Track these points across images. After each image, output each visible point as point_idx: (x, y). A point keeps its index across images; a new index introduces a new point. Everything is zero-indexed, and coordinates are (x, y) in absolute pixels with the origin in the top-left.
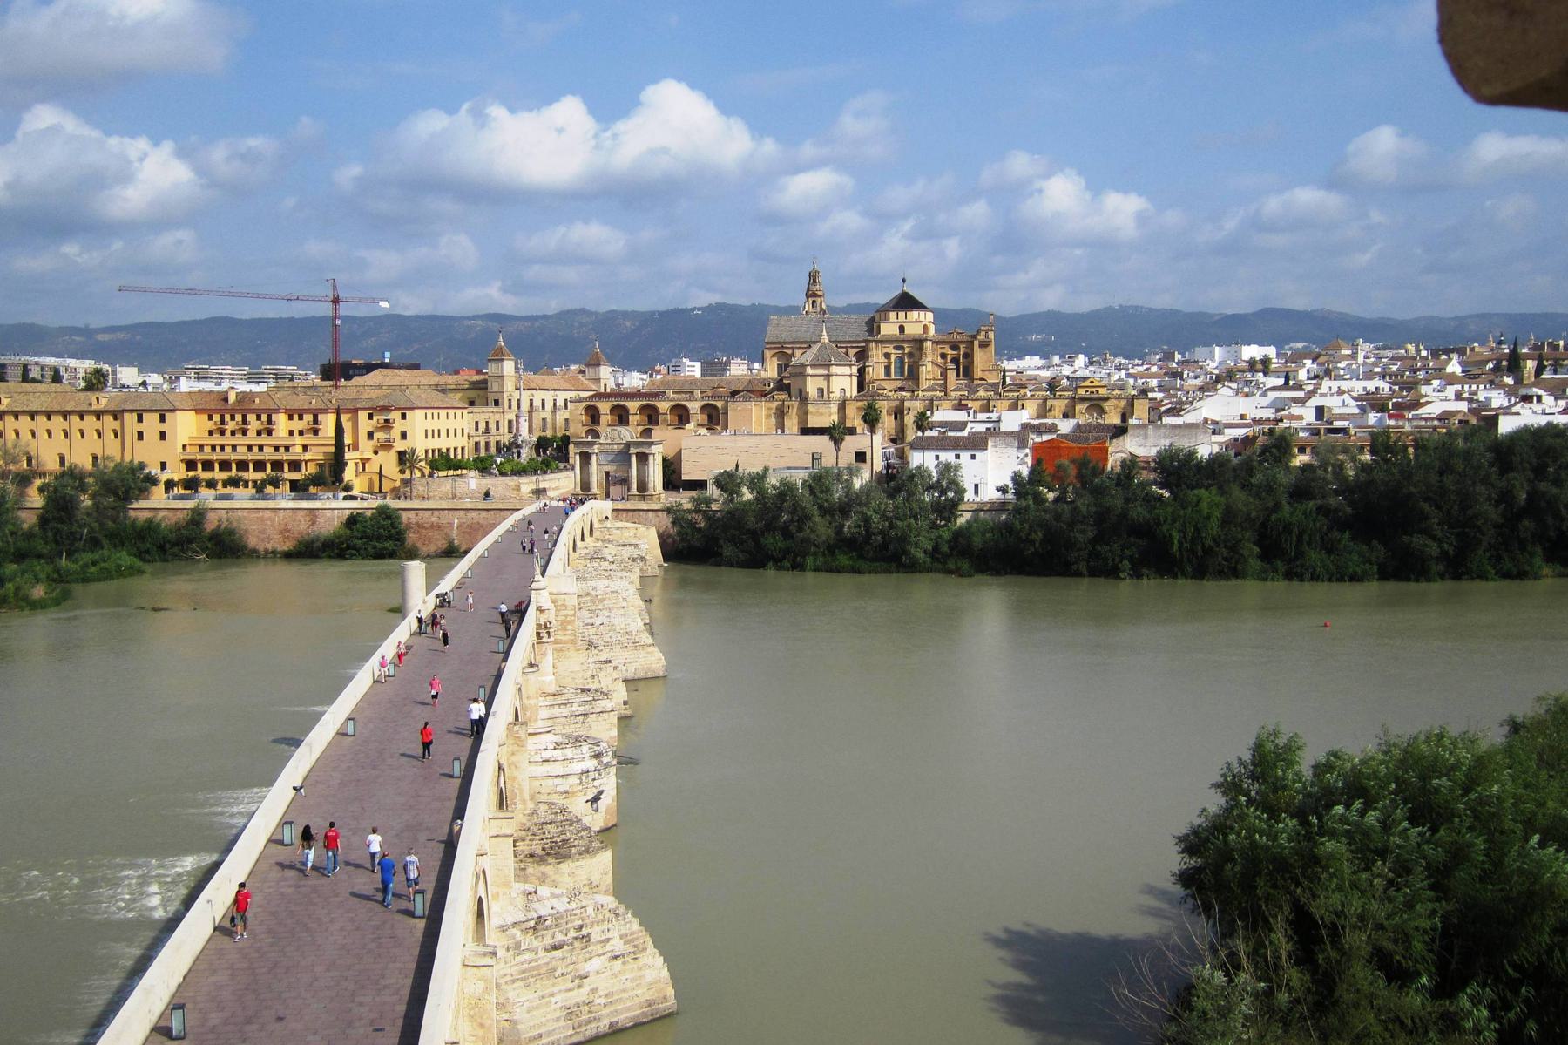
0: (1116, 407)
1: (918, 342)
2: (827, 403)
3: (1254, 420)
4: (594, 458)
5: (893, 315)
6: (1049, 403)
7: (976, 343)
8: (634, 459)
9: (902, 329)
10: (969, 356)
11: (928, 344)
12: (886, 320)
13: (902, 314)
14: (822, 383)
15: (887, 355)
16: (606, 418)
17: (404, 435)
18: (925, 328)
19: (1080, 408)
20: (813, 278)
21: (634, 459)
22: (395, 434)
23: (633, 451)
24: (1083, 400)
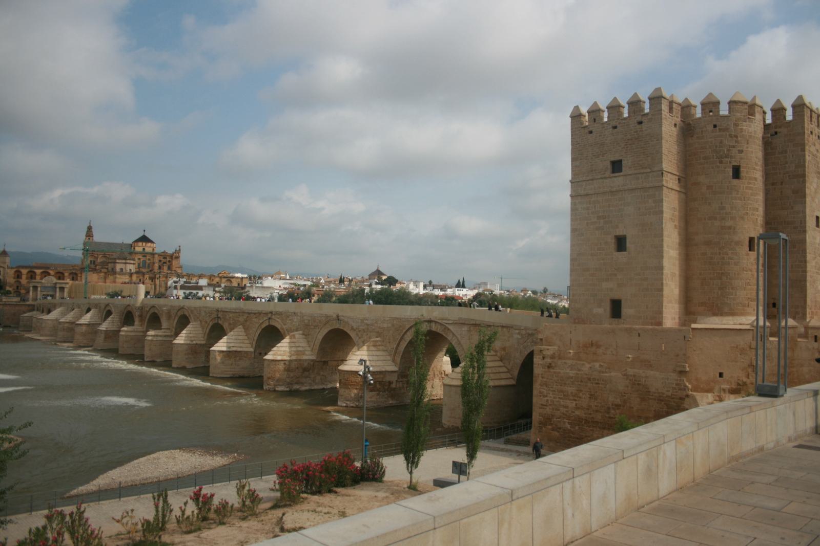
0: (236, 281)
3: (284, 288)
4: (39, 289)
5: (140, 244)
7: (174, 257)
8: (58, 290)
9: (144, 249)
13: (144, 244)
14: (122, 266)
15: (139, 259)
16: (24, 277)
19: (224, 280)
20: (90, 228)
21: (58, 290)
23: (58, 286)
24: (224, 277)
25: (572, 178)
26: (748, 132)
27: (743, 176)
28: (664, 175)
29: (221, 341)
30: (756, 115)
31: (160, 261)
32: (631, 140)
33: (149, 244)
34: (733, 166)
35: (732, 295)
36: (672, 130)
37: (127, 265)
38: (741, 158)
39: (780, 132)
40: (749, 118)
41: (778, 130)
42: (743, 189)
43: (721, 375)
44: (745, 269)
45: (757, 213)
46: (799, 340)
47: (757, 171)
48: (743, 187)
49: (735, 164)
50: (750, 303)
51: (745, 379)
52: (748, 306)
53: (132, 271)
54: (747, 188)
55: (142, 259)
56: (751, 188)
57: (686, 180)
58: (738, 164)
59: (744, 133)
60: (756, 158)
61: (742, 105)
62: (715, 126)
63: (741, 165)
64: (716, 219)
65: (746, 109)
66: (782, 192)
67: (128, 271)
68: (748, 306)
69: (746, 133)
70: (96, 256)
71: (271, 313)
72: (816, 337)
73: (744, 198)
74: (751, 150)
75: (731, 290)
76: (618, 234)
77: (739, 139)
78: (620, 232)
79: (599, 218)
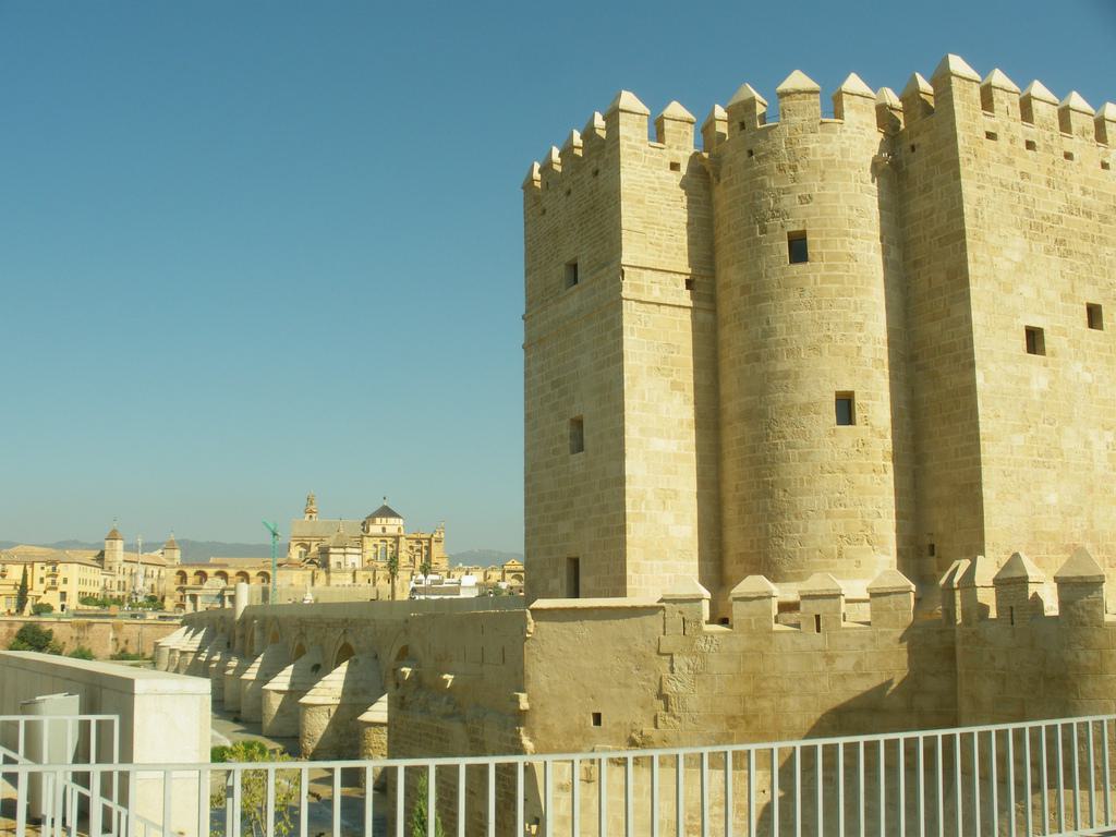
1: (397, 539)
2: (344, 572)
5: (378, 520)
6: (488, 574)
7: (433, 539)
8: (227, 599)
9: (384, 529)
10: (429, 548)
11: (402, 539)
12: (374, 522)
13: (384, 520)
14: (340, 558)
15: (375, 546)
17: (65, 581)
18: (399, 529)
19: (508, 576)
20: (310, 501)
21: (227, 599)
22: (59, 580)
23: (227, 593)
24: (509, 572)
25: (527, 312)
26: (822, 155)
27: (813, 255)
28: (625, 275)
29: (283, 673)
30: (845, 114)
31: (411, 548)
32: (586, 211)
33: (392, 520)
34: (788, 233)
35: (798, 532)
36: (658, 178)
37: (347, 556)
38: (807, 215)
39: (919, 145)
40: (822, 123)
41: (916, 141)
42: (815, 283)
43: (597, 719)
44: (827, 467)
45: (859, 334)
46: (776, 627)
47: (855, 237)
48: (815, 277)
49: (795, 228)
50: (846, 547)
51: (648, 729)
52: (840, 555)
53: (357, 566)
54: (824, 279)
55: (381, 545)
56: (839, 280)
57: (704, 283)
58: (801, 229)
59: (811, 158)
60: (851, 208)
61: (805, 98)
62: (751, 153)
63: (807, 229)
64: (758, 359)
65: (814, 104)
66: (930, 280)
67: (350, 566)
68: (840, 555)
69: (819, 157)
70: (308, 543)
71: (346, 620)
72: (818, 617)
73: (819, 302)
74: (834, 192)
75: (794, 521)
76: (573, 416)
77: (800, 170)
78: (575, 414)
79: (555, 384)
